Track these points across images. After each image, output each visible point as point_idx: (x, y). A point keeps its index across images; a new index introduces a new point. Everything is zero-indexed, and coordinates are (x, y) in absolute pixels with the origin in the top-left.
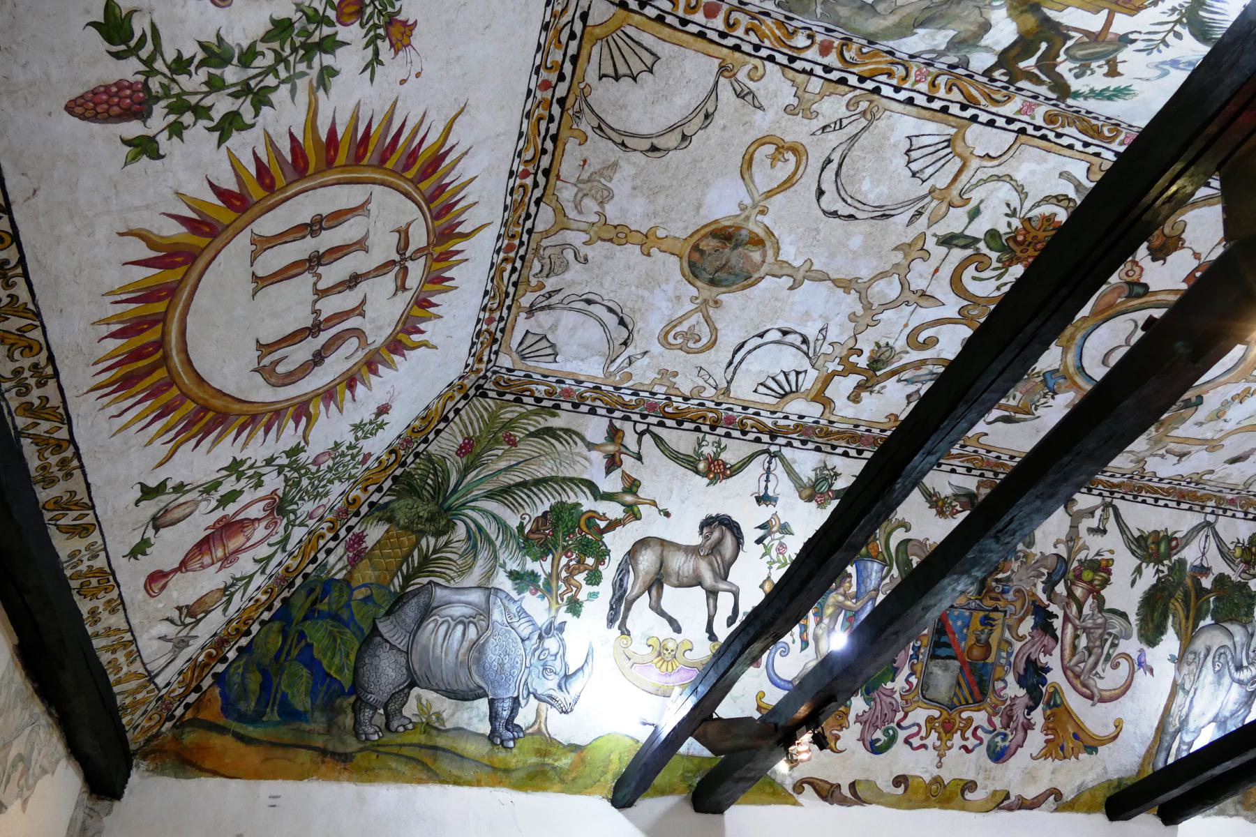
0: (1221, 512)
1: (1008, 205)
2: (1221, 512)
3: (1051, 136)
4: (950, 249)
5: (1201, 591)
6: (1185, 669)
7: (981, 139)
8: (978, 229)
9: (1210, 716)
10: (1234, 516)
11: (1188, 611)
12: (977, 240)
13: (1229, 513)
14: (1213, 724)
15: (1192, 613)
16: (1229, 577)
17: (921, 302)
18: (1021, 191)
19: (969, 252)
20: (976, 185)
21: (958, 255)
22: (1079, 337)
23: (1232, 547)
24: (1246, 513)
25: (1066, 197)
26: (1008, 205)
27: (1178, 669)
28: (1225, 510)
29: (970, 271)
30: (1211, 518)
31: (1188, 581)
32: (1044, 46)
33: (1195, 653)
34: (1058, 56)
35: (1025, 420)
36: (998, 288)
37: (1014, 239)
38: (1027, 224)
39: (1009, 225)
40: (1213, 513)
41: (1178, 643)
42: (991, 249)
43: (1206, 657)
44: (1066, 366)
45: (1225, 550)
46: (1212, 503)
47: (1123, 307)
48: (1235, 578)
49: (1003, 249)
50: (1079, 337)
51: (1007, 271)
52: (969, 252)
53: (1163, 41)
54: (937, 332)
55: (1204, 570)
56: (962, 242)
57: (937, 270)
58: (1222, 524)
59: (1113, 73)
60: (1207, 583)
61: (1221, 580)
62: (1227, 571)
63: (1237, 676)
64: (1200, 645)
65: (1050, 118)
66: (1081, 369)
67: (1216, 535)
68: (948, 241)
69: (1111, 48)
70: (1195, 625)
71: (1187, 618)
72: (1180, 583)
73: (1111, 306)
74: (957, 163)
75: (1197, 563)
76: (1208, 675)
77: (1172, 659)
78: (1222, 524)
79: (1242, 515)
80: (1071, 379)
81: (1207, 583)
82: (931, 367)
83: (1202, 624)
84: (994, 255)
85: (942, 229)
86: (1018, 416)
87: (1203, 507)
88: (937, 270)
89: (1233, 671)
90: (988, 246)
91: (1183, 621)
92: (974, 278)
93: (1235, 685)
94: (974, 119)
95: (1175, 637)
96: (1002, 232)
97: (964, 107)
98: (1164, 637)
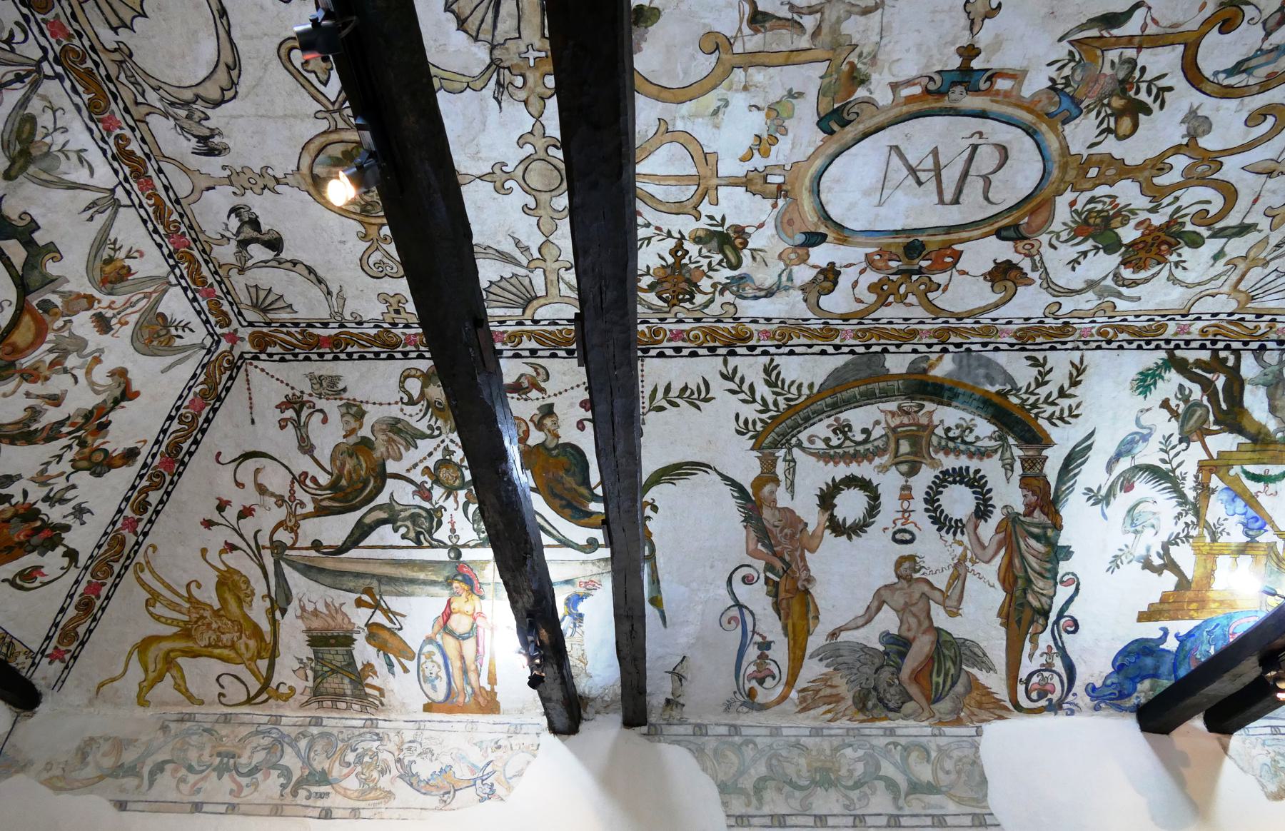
1: (1184, 268)
3: (1157, 318)
4: (1242, 223)
7: (1224, 304)
8: (1212, 246)
12: (1211, 237)
17: (1273, 165)
18: (1172, 279)
19: (1218, 226)
20: (1220, 275)
21: (1233, 220)
22: (1055, 173)
25: (1128, 286)
26: (1184, 268)
29: (1214, 210)
32: (1224, 406)
34: (1209, 401)
35: (1081, 28)
36: (1177, 199)
37: (1170, 245)
38: (1160, 259)
39: (1180, 255)
42: (1195, 232)
44: (1054, 130)
47: (1016, 214)
49: (1181, 234)
50: (1055, 173)
51: (1171, 216)
52: (1218, 226)
53: (1166, 452)
54: (1247, 134)
56: (1228, 232)
57: (1255, 201)
59: (1165, 404)
65: (1163, 327)
66: (1031, 132)
68: (1243, 229)
69: (1187, 428)
73: (1032, 213)
74: (1242, 287)
80: (1038, 116)
82: (1252, 81)
84: (1189, 227)
85: (1252, 238)
86: (1094, 33)
88: (1255, 201)
90: (1198, 234)
92: (1209, 202)
94: (1230, 314)
96: (1186, 248)
97: (1243, 319)
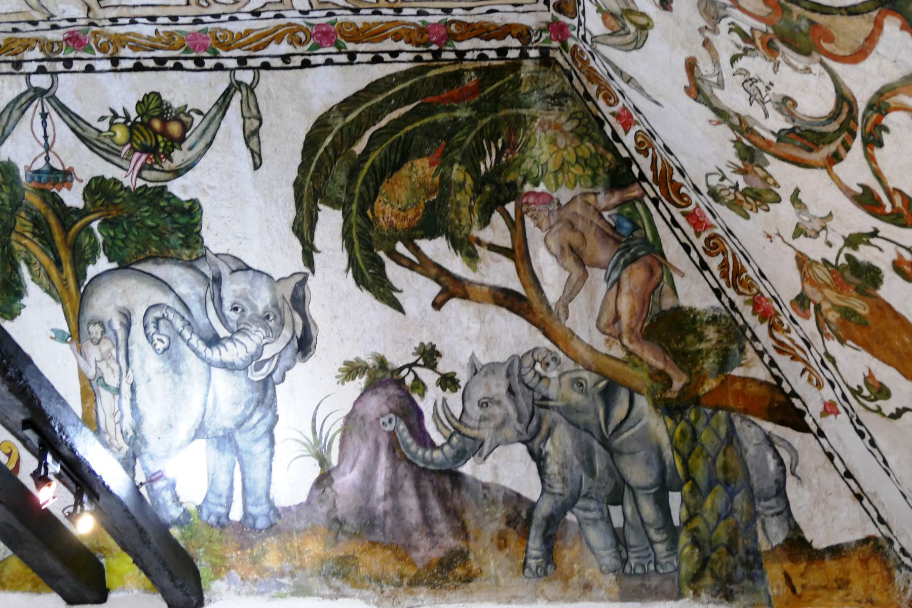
0: (60, 66)
2: (60, 66)
5: (65, 214)
6: (94, 353)
9: (186, 424)
10: (90, 69)
11: (55, 252)
13: (78, 66)
14: (201, 443)
15: (64, 255)
16: (116, 182)
23: (104, 126)
24: (115, 61)
27: (81, 352)
28: (68, 63)
30: (41, 81)
31: (33, 200)
33: (101, 324)
40: (41, 70)
41: (59, 307)
43: (128, 327)
45: (91, 134)
46: (37, 53)
48: (129, 180)
55: (65, 176)
58: (70, 88)
60: (73, 197)
61: (99, 189)
62: (109, 171)
63: (214, 354)
64: (106, 303)
67: (63, 110)
70: (80, 275)
71: (58, 263)
72: (17, 203)
75: (40, 164)
76: (147, 359)
77: (59, 336)
78: (70, 88)
79: (107, 65)
81: (73, 197)
83: (92, 271)
87: (18, 65)
89: (201, 347)
91: (53, 271)
93: (217, 373)
95: (47, 298)
98: (24, 301)
